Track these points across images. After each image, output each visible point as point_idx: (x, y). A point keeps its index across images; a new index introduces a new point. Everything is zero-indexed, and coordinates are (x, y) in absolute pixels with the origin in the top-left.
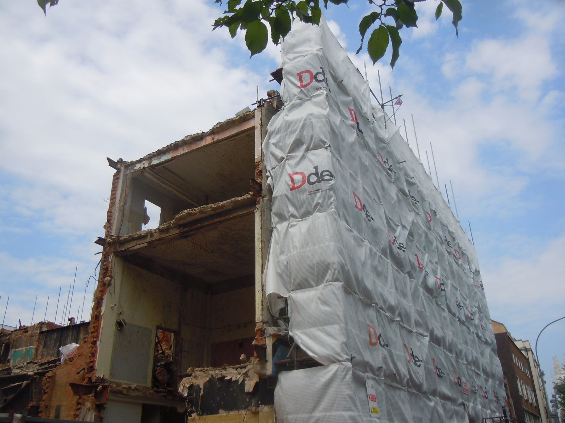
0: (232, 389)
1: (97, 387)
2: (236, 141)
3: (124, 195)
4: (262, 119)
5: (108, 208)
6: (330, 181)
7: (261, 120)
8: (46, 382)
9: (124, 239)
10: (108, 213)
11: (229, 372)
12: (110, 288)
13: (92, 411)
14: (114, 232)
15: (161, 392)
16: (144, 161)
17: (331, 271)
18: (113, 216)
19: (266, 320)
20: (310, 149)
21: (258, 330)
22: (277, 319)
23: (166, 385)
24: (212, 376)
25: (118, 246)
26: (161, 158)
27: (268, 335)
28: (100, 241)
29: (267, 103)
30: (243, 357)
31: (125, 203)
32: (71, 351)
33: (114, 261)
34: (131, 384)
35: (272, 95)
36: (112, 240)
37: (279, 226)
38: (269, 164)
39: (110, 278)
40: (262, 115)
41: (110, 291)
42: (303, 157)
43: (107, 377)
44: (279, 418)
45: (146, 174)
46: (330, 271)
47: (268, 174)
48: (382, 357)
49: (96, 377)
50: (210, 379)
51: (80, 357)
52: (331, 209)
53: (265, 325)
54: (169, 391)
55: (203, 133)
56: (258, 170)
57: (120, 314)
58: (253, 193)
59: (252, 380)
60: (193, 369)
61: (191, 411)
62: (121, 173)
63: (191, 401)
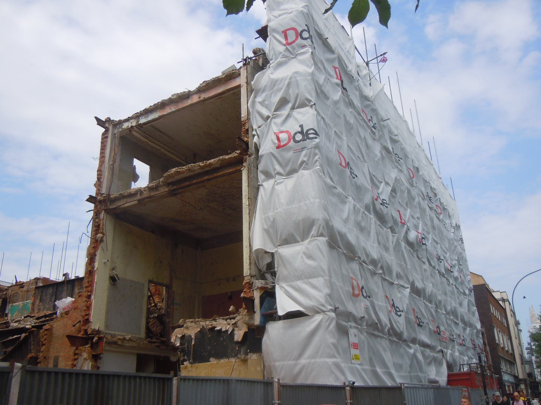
0: (222, 339)
1: (93, 338)
2: (222, 98)
3: (113, 154)
4: (248, 77)
5: (98, 167)
6: (315, 140)
7: (247, 78)
8: (43, 335)
9: (114, 197)
10: (97, 172)
11: (219, 323)
12: (102, 244)
13: (89, 361)
14: (104, 191)
15: (155, 342)
16: (132, 119)
17: (317, 227)
18: (103, 175)
19: (254, 273)
20: (295, 108)
21: (246, 284)
22: (264, 273)
23: (159, 335)
24: (203, 327)
25: (108, 204)
26: (148, 117)
27: (256, 288)
28: (91, 199)
29: (252, 61)
30: (232, 309)
31: (114, 162)
32: (67, 305)
33: (105, 218)
34: (125, 336)
35: (258, 52)
36: (102, 198)
37: (265, 184)
38: (256, 122)
39: (102, 235)
40: (248, 73)
41: (102, 247)
42: (288, 116)
43: (102, 329)
44: (266, 365)
45: (134, 133)
46: (314, 227)
47: (254, 133)
48: (365, 307)
49: (91, 329)
50: (201, 329)
51: (75, 310)
52: (316, 167)
53: (252, 278)
54: (162, 341)
55: (189, 91)
56: (244, 128)
57: (113, 269)
58: (240, 151)
59: (241, 330)
60: (185, 321)
61: (184, 359)
62: (109, 132)
63: (183, 351)
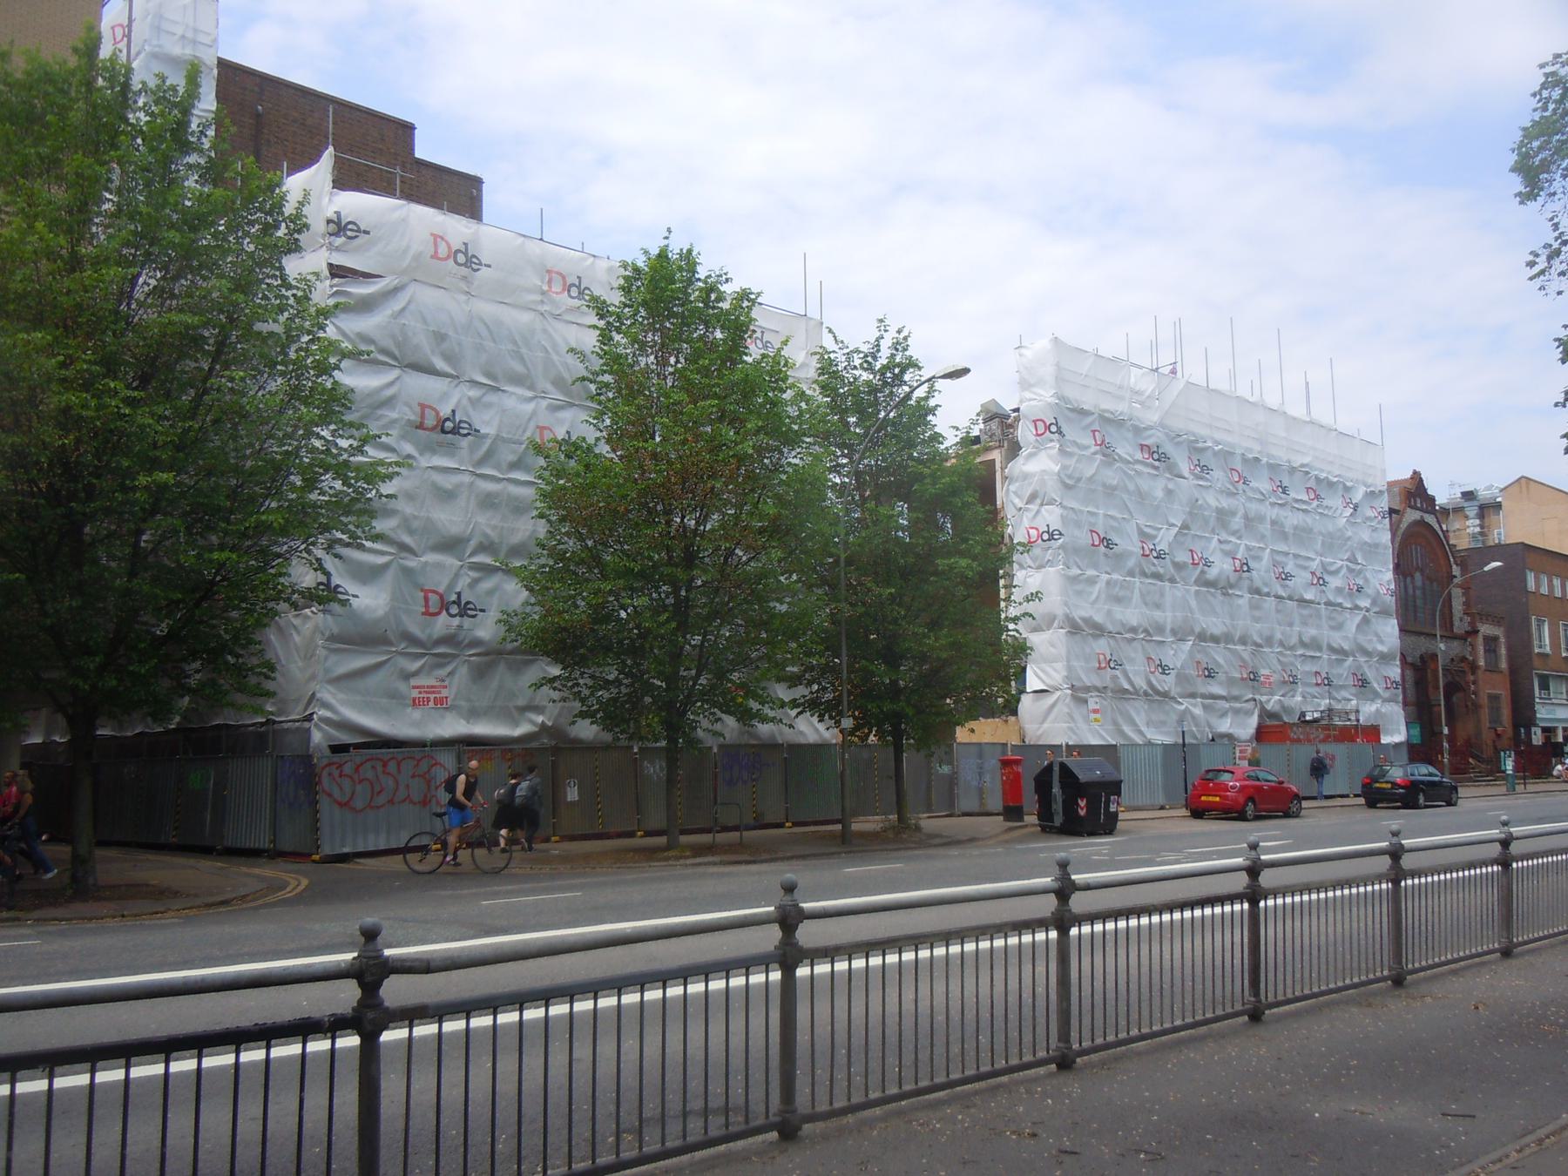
38: (1009, 512)
